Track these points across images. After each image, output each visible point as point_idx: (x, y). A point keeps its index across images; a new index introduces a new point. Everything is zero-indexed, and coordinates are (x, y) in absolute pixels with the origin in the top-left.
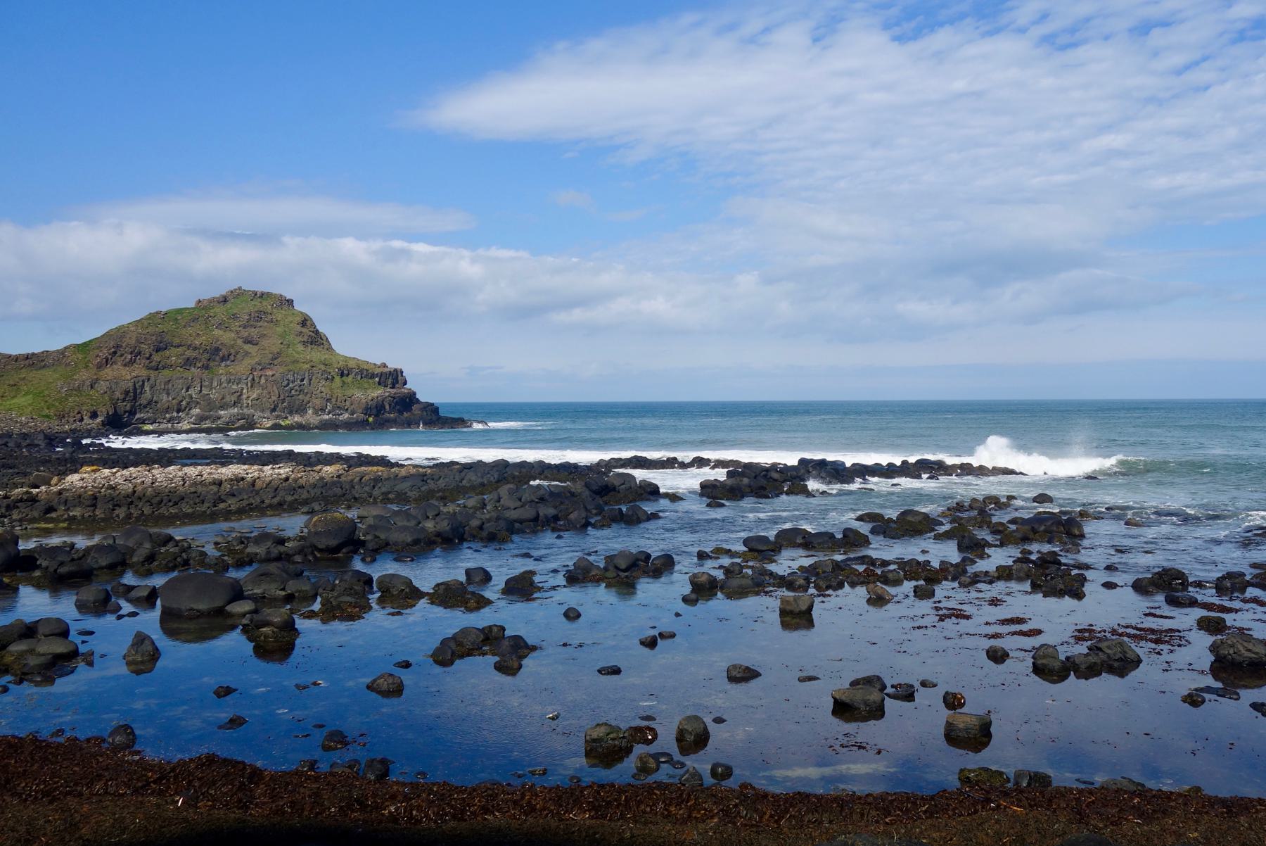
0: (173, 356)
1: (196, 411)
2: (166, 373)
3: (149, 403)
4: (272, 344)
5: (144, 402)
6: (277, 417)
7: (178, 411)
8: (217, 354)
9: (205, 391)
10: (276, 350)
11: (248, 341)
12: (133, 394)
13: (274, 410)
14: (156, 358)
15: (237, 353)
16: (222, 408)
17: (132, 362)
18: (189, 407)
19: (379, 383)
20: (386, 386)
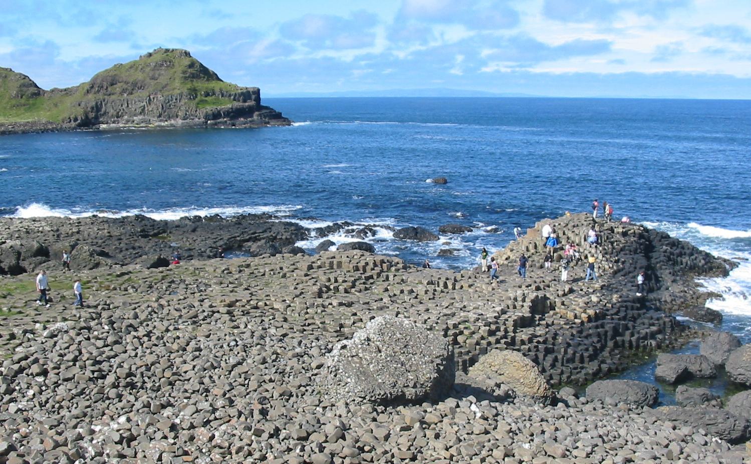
0: (118, 88)
1: (126, 117)
2: (113, 97)
3: (105, 113)
4: (163, 80)
5: (102, 112)
6: (161, 121)
7: (117, 117)
8: (136, 86)
9: (130, 106)
10: (164, 83)
11: (153, 78)
12: (97, 108)
13: (160, 116)
14: (109, 89)
15: (145, 85)
16: (135, 115)
17: (98, 91)
18: (122, 116)
19: (234, 100)
20: (239, 101)
